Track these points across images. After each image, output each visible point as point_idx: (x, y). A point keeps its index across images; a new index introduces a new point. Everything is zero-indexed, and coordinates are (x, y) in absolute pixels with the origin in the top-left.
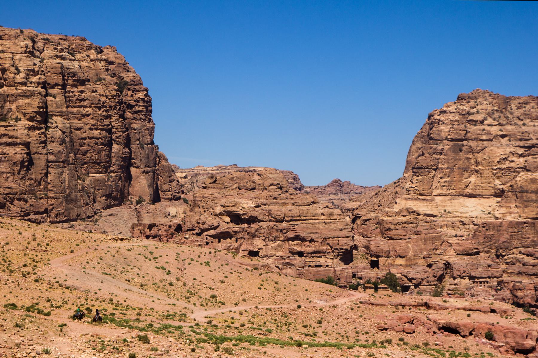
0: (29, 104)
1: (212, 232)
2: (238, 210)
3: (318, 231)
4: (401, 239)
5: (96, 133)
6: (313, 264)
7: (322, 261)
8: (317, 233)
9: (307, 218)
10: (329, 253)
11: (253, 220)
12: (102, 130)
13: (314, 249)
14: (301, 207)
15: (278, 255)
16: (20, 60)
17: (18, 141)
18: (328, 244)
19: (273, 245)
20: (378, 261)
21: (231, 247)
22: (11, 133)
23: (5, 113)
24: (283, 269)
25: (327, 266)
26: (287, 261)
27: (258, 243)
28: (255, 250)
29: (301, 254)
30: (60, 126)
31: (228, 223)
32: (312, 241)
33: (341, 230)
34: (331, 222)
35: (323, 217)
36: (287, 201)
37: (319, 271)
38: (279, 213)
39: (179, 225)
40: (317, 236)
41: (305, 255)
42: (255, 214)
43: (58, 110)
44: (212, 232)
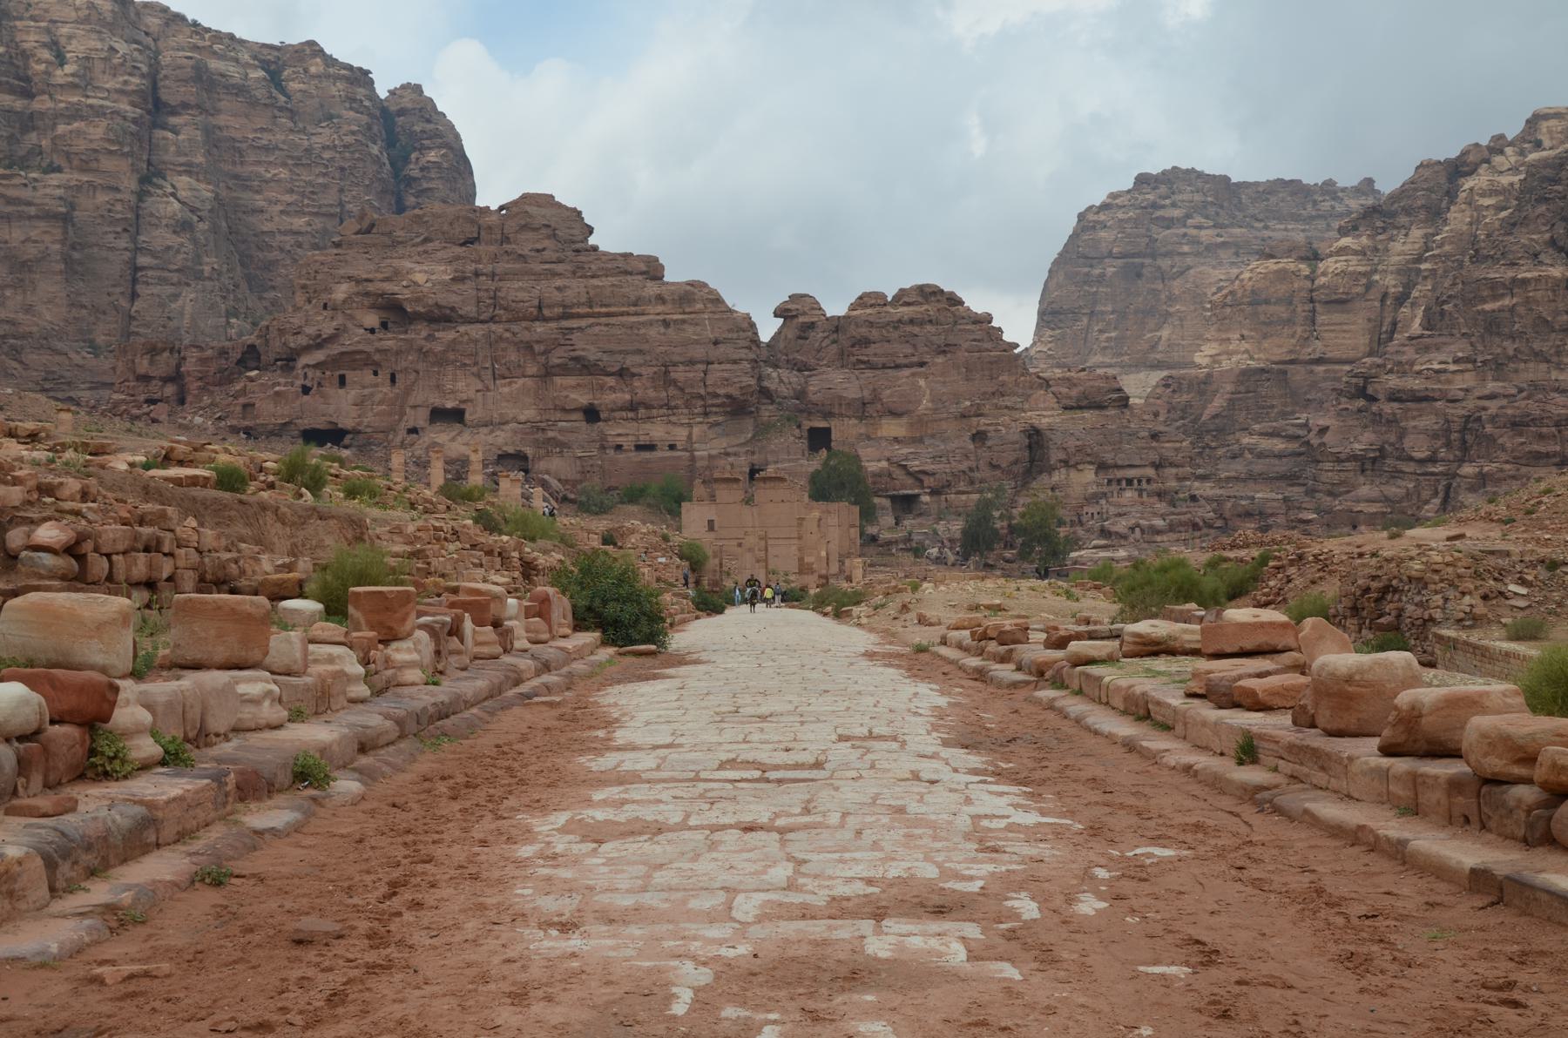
0: (78, 132)
1: (319, 356)
2: (396, 289)
3: (645, 347)
4: (897, 367)
5: (299, 222)
6: (627, 442)
7: (657, 431)
8: (640, 352)
9: (612, 309)
10: (676, 407)
11: (442, 317)
12: (316, 214)
13: (628, 397)
14: (595, 282)
15: (522, 418)
16: (70, 38)
17: (32, 210)
18: (674, 382)
19: (506, 390)
20: (828, 431)
21: (378, 397)
22: (11, 193)
23: (22, 153)
24: (540, 459)
25: (672, 447)
26: (550, 434)
27: (461, 385)
28: (449, 405)
29: (591, 414)
30: (182, 194)
31: (372, 331)
32: (622, 373)
33: (716, 343)
34: (684, 321)
35: (660, 308)
36: (560, 268)
37: (648, 461)
38: (522, 295)
39: (252, 347)
40: (638, 359)
41: (602, 416)
42: (453, 299)
43: (182, 159)
44: (319, 356)
